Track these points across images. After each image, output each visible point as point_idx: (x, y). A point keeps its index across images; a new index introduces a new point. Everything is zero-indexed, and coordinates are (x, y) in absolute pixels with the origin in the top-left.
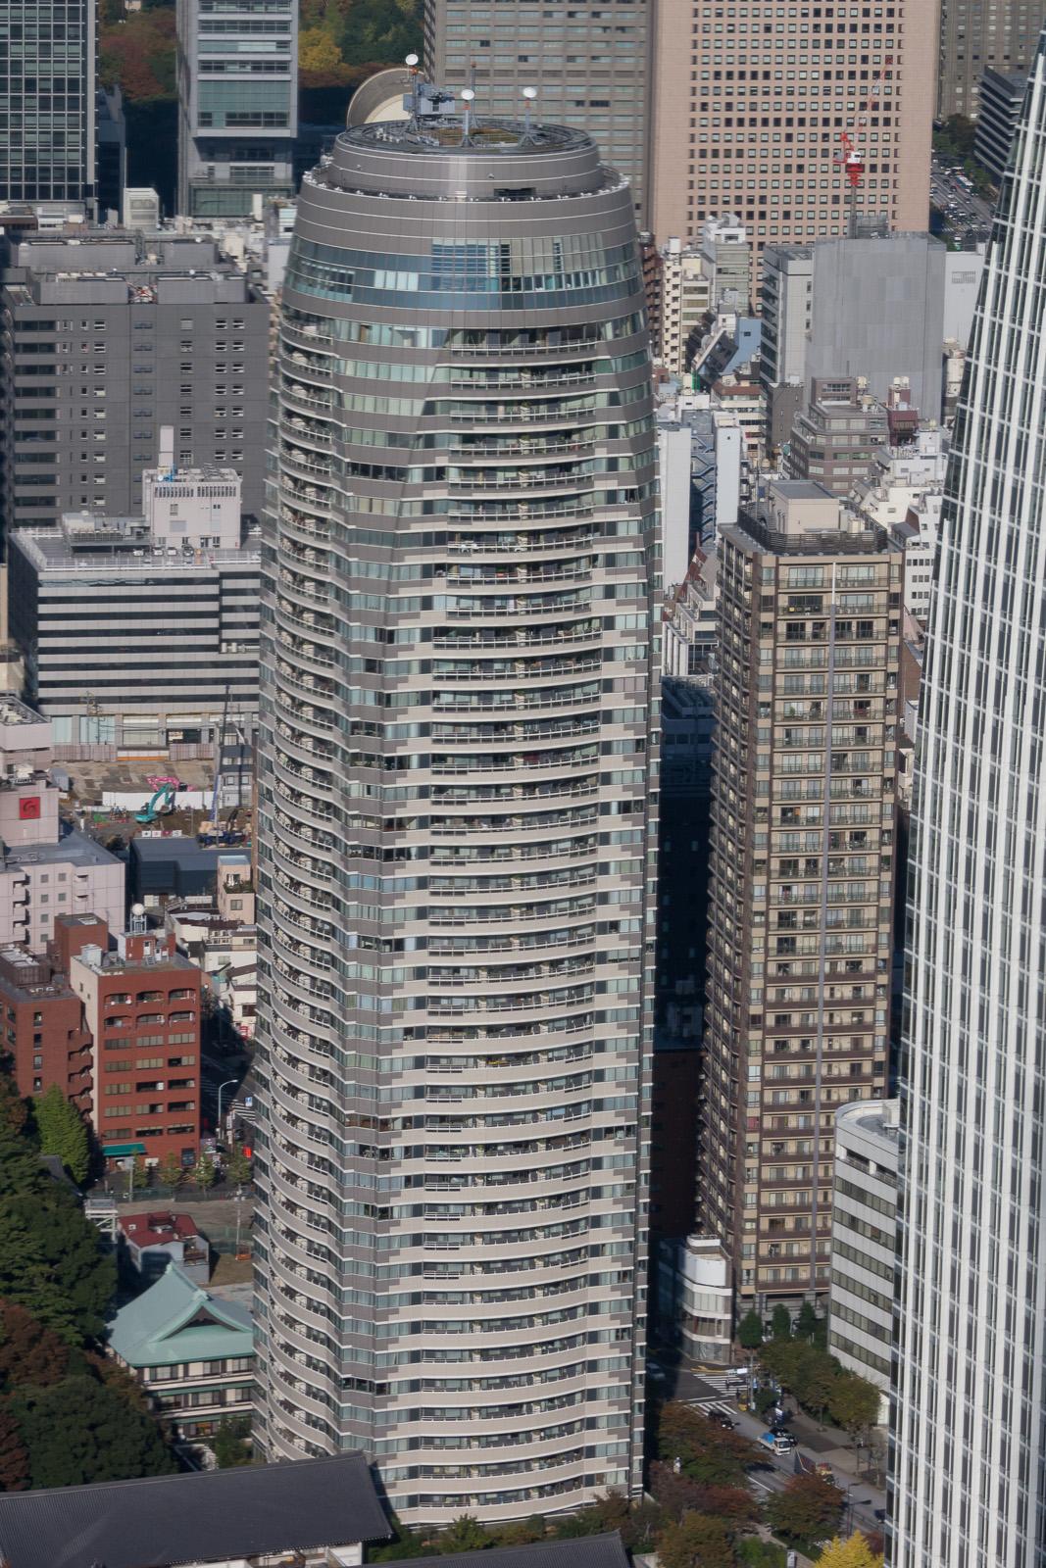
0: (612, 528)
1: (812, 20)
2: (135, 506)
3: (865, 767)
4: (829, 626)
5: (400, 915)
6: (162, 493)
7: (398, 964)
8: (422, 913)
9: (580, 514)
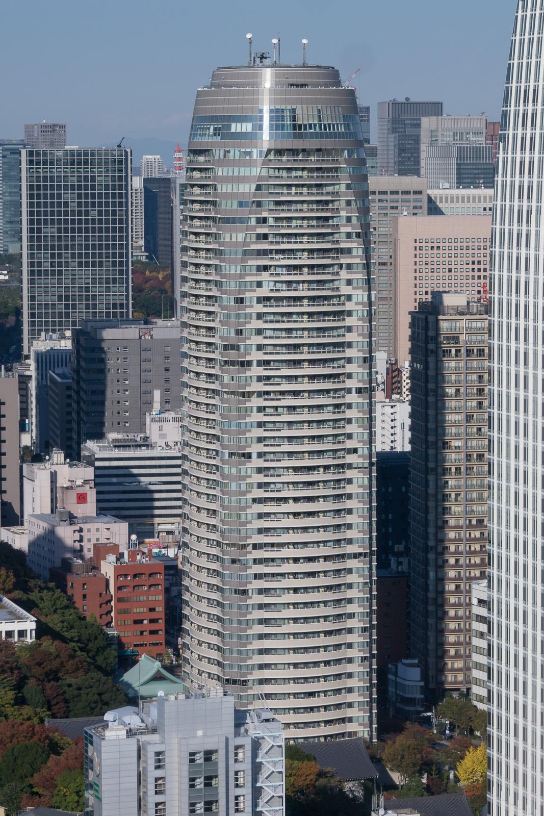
0: (349, 251)
1: (471, 266)
2: (142, 427)
3: (483, 420)
4: (463, 351)
5: (249, 440)
6: (153, 420)
7: (248, 465)
8: (260, 440)
9: (333, 242)
